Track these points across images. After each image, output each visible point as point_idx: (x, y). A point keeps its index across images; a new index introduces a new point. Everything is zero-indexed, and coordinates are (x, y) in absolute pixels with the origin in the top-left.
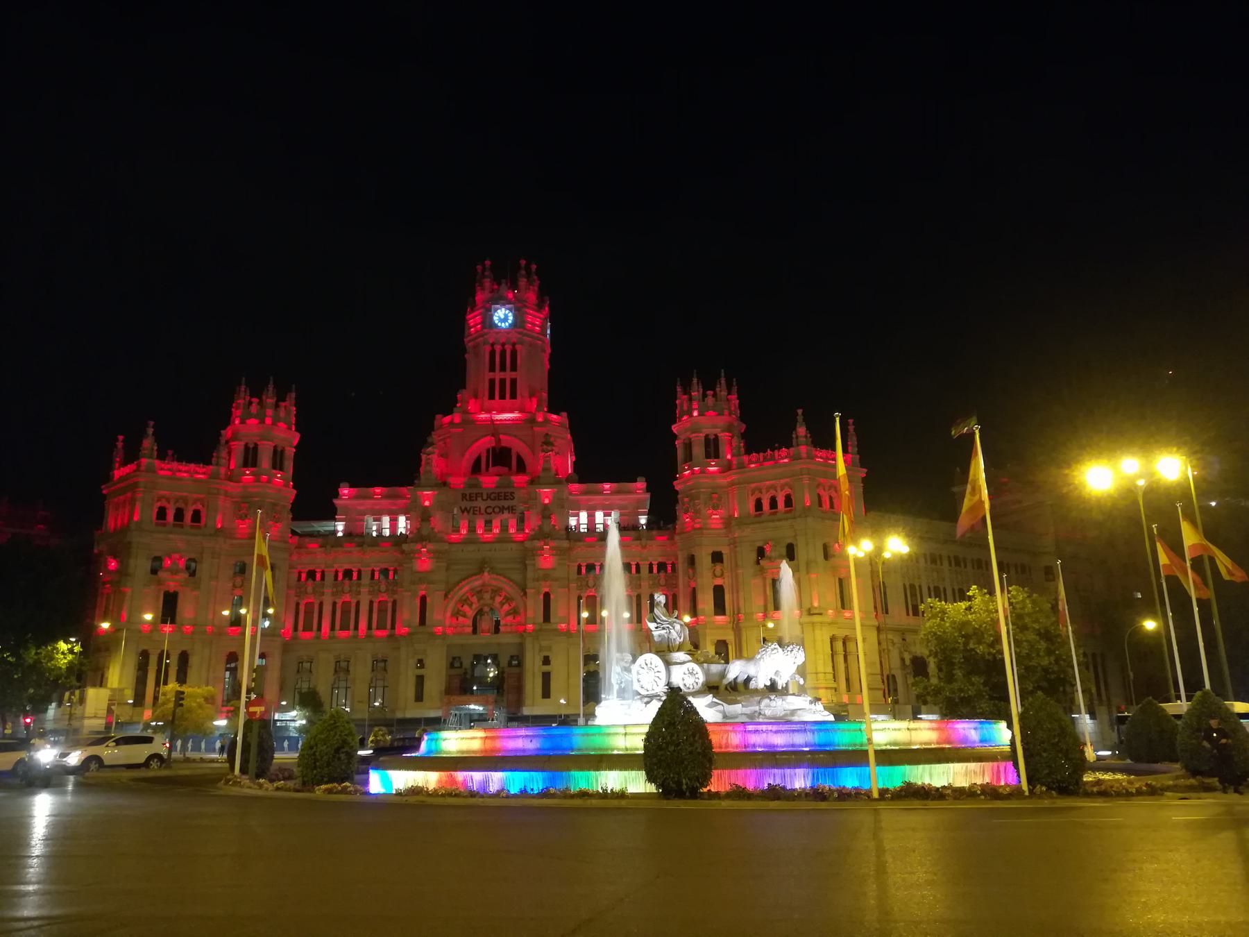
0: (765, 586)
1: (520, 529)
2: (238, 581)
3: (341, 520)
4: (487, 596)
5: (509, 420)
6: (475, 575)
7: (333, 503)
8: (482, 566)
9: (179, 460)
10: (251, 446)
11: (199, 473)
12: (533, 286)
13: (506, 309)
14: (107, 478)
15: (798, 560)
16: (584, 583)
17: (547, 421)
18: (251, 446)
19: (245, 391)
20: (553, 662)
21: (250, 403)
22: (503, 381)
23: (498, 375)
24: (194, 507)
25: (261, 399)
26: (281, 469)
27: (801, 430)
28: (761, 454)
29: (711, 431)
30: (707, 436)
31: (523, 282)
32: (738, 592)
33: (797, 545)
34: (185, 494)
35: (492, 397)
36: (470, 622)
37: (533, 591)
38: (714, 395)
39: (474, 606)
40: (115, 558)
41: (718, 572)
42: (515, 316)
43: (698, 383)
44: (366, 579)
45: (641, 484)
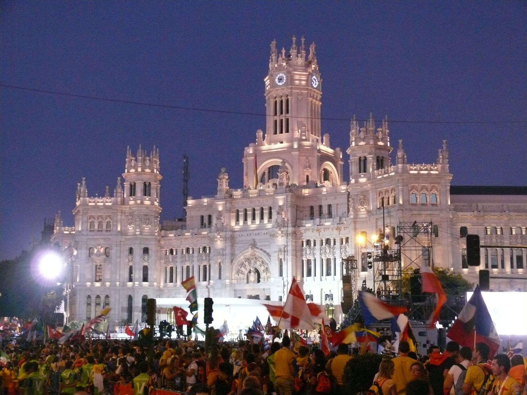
2: (130, 257)
4: (252, 261)
5: (283, 148)
9: (99, 197)
10: (133, 184)
11: (107, 202)
13: (282, 73)
14: (74, 206)
18: (133, 184)
21: (132, 160)
22: (282, 121)
23: (278, 118)
24: (107, 220)
25: (135, 156)
29: (362, 155)
31: (293, 52)
35: (275, 133)
36: (245, 277)
42: (287, 77)
43: (356, 124)
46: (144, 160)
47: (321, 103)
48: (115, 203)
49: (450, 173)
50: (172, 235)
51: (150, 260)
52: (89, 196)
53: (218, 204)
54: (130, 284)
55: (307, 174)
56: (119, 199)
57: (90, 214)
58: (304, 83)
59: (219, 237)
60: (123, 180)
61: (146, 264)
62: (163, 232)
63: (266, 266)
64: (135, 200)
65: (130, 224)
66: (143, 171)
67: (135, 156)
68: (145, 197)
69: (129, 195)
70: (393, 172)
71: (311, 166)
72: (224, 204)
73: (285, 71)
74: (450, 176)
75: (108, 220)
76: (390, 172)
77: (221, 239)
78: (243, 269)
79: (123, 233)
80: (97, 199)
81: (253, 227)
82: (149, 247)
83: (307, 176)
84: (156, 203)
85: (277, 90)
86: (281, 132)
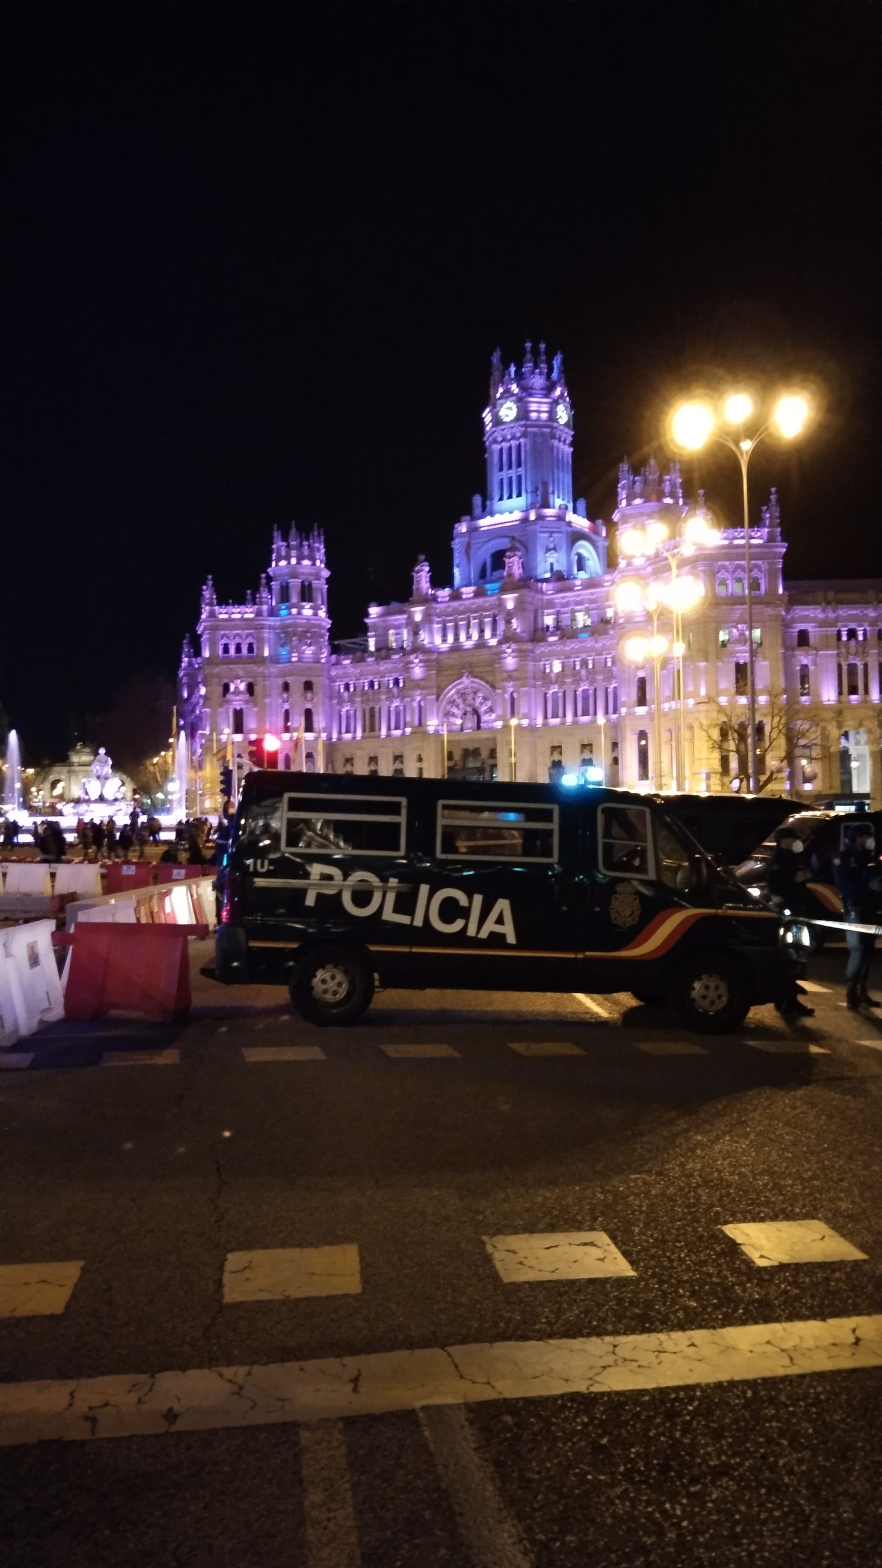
1: (494, 635)
2: (285, 695)
3: (372, 637)
7: (366, 624)
9: (233, 604)
10: (284, 584)
12: (540, 368)
17: (540, 517)
18: (284, 584)
22: (510, 479)
23: (505, 474)
26: (310, 600)
31: (528, 367)
34: (239, 632)
38: (645, 482)
39: (461, 706)
44: (383, 690)
46: (301, 546)
47: (571, 449)
48: (259, 614)
49: (782, 541)
50: (347, 662)
51: (315, 700)
52: (220, 604)
53: (414, 612)
55: (551, 560)
56: (265, 607)
57: (222, 632)
58: (544, 416)
60: (269, 579)
61: (309, 706)
62: (334, 657)
64: (289, 608)
66: (298, 563)
68: (304, 604)
71: (558, 548)
73: (514, 398)
74: (782, 547)
75: (250, 640)
77: (420, 665)
78: (455, 710)
80: (231, 609)
81: (468, 644)
82: (314, 680)
83: (552, 564)
84: (322, 613)
85: (503, 430)
86: (510, 497)
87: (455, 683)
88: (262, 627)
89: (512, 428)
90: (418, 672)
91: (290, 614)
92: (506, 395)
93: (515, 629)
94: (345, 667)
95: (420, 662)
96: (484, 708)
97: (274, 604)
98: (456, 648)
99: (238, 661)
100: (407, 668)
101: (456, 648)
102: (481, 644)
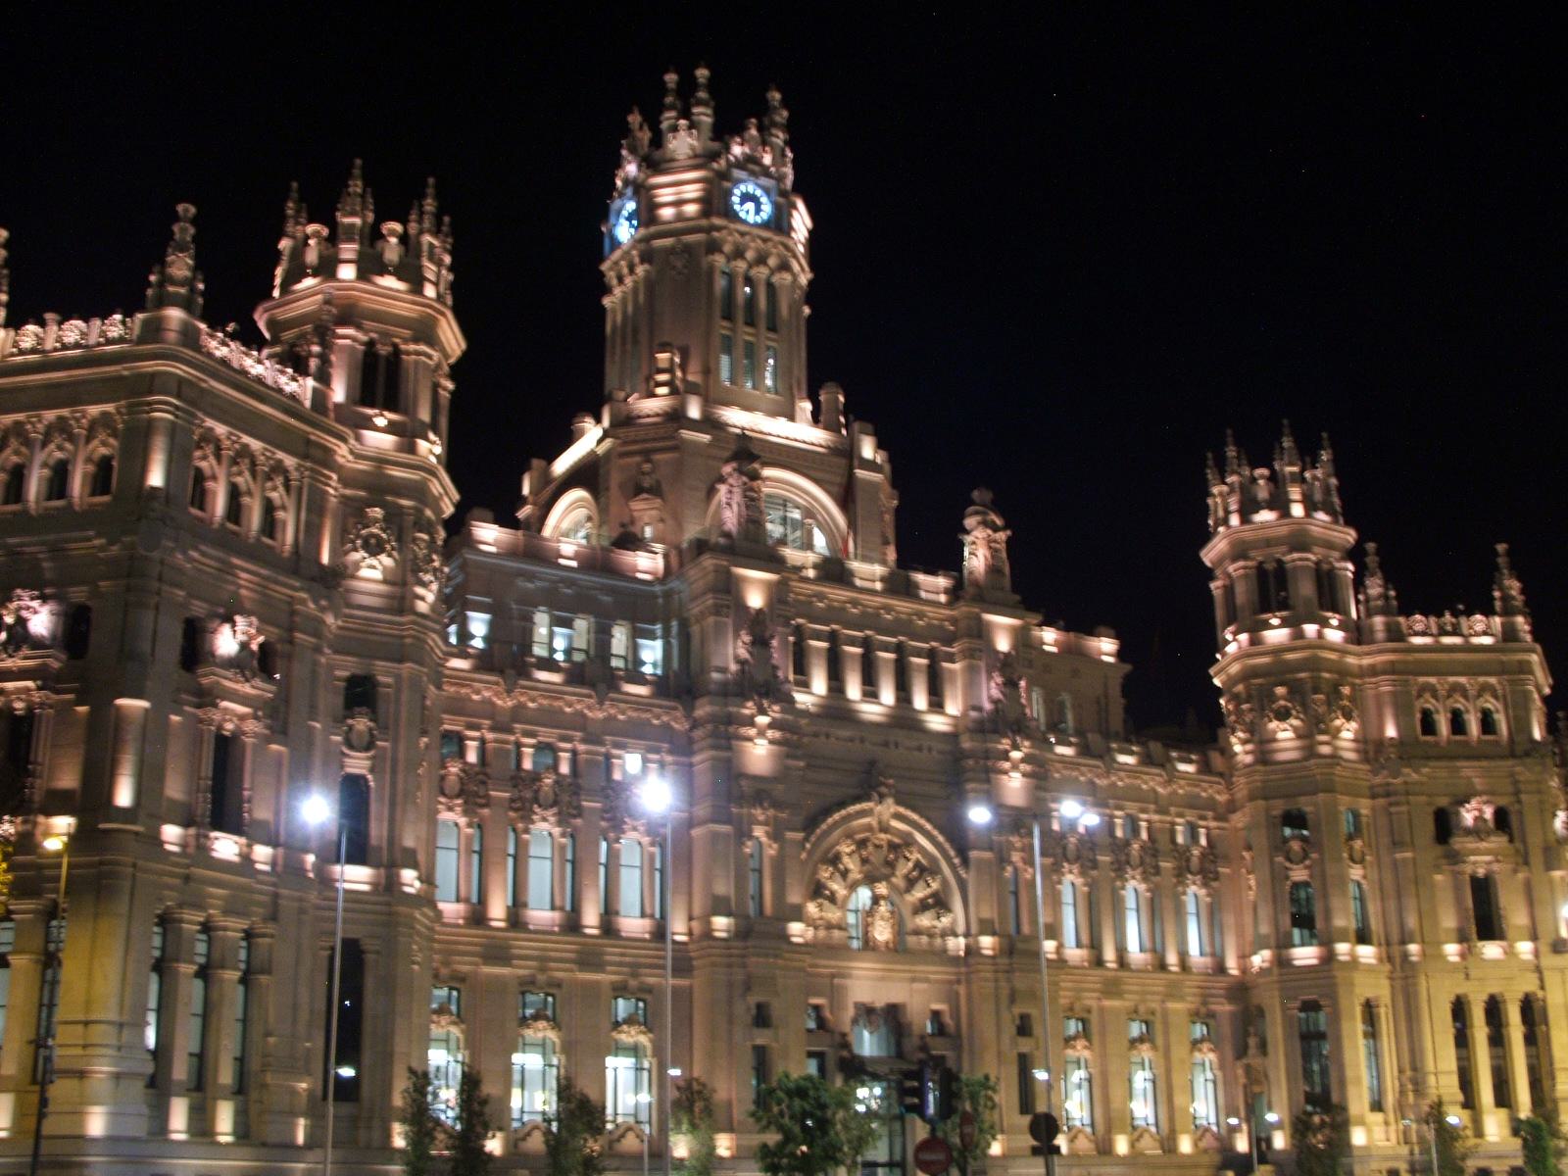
0: (1457, 889)
1: (937, 704)
2: (362, 724)
6: (858, 799)
8: (867, 783)
10: (384, 350)
15: (1524, 842)
16: (1059, 851)
18: (384, 350)
19: (363, 196)
20: (1037, 1030)
27: (1514, 586)
28: (1433, 620)
30: (1318, 563)
32: (1399, 897)
33: (1520, 813)
37: (987, 855)
40: (44, 599)
41: (1357, 856)
45: (1106, 647)
52: (203, 319)
53: (744, 579)
54: (356, 877)
59: (762, 720)
63: (935, 885)
64: (407, 434)
65: (366, 547)
67: (404, 222)
69: (357, 396)
70: (1485, 633)
72: (769, 585)
76: (1465, 631)
77: (770, 733)
79: (333, 580)
85: (742, 234)
87: (852, 809)
88: (326, 459)
89: (765, 240)
90: (759, 753)
91: (412, 449)
92: (751, 166)
93: (1023, 706)
94: (459, 678)
95: (771, 726)
96: (919, 893)
97: (338, 394)
98: (837, 709)
99: (257, 553)
100: (726, 734)
101: (837, 709)
102: (903, 718)
